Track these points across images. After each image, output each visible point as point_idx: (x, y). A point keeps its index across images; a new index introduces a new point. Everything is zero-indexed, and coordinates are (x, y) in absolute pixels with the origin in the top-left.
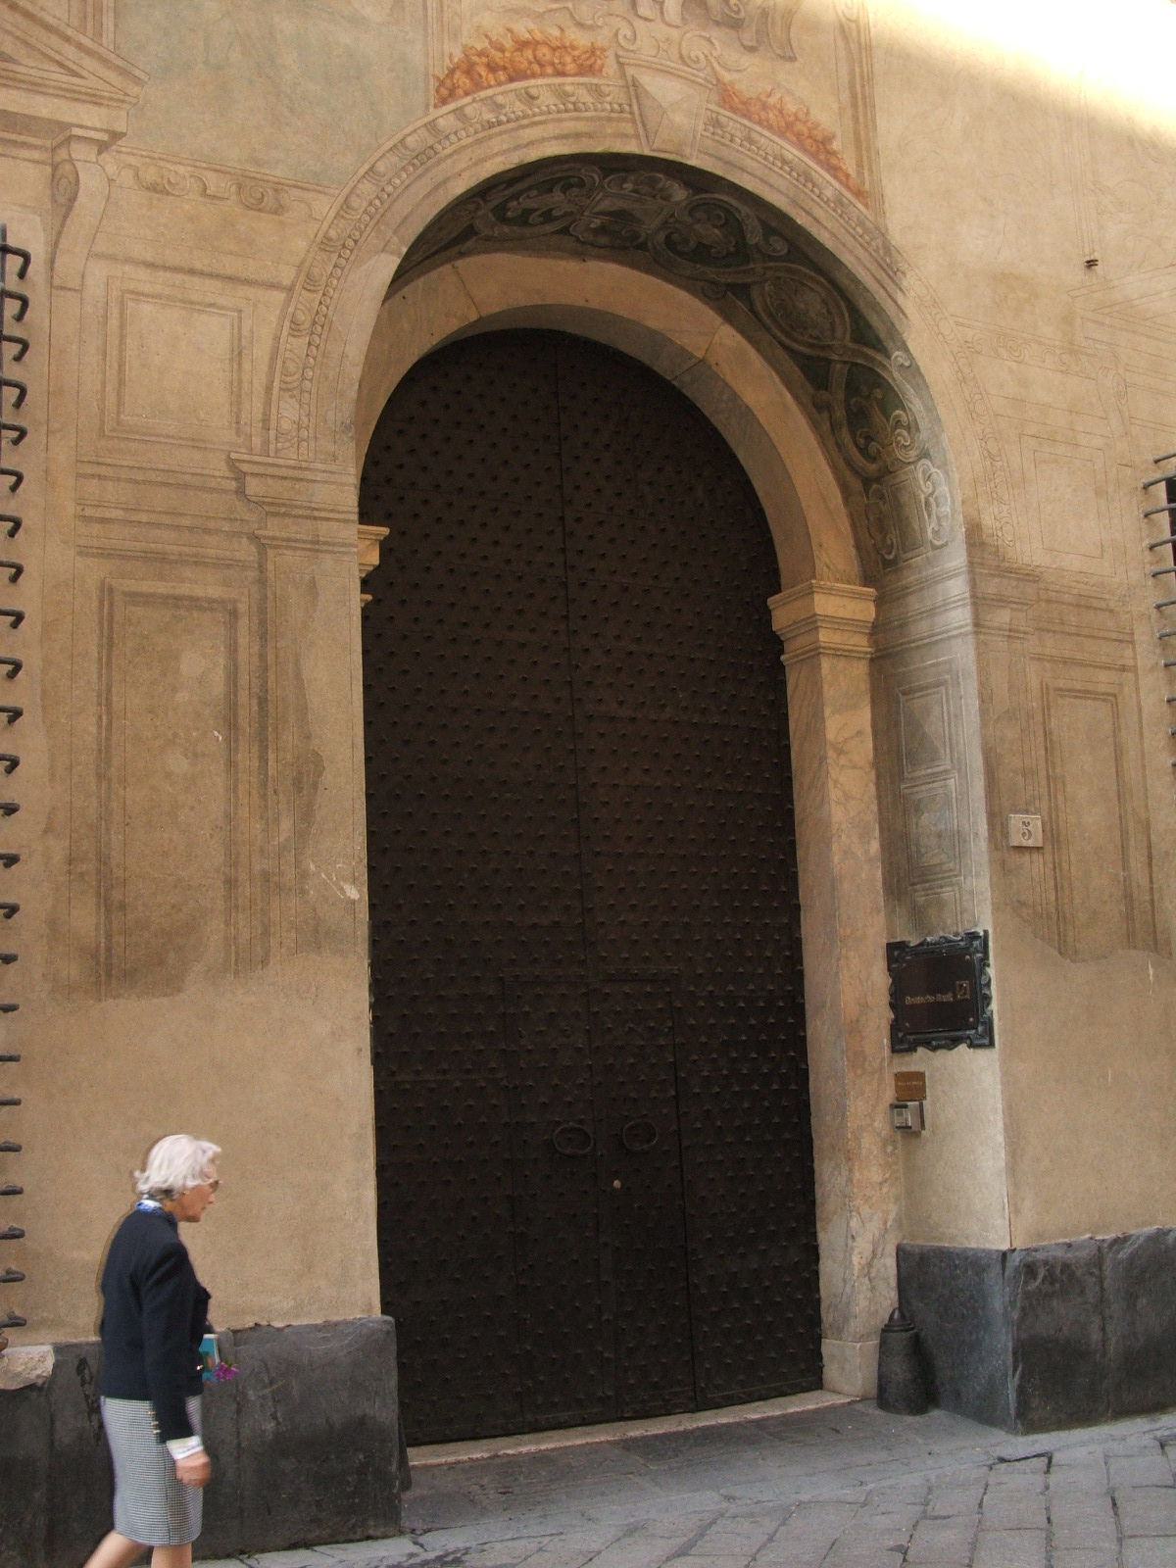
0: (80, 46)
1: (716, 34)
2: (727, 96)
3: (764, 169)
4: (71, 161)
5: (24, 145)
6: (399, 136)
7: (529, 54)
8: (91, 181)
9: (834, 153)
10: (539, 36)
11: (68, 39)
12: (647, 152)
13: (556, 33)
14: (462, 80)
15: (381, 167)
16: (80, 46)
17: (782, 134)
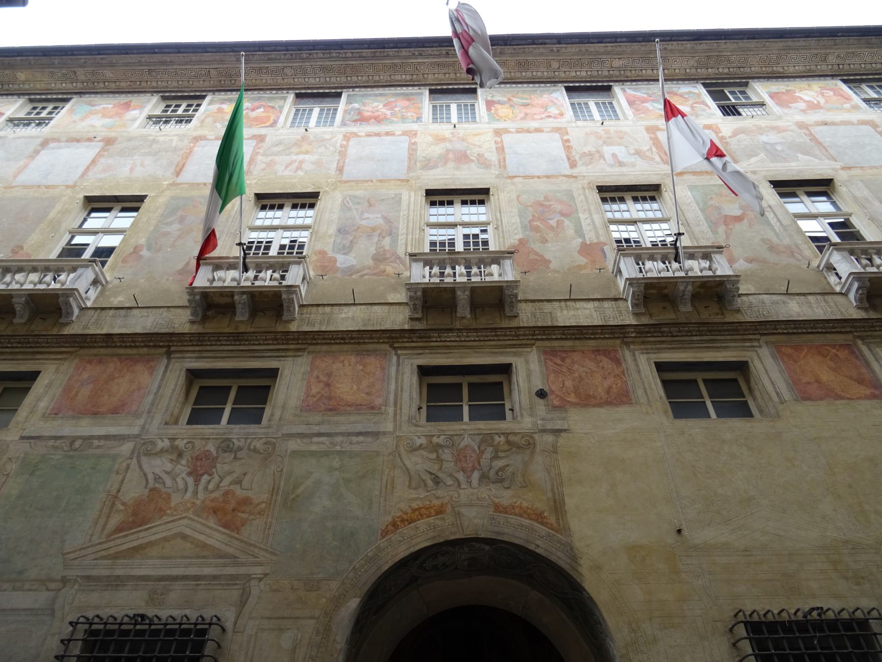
1: (492, 486)
2: (497, 508)
3: (515, 531)
5: (236, 584)
7: (417, 513)
8: (255, 592)
9: (545, 517)
10: (421, 506)
11: (256, 547)
12: (463, 537)
13: (428, 503)
14: (390, 527)
15: (357, 566)
16: (260, 548)
17: (521, 516)
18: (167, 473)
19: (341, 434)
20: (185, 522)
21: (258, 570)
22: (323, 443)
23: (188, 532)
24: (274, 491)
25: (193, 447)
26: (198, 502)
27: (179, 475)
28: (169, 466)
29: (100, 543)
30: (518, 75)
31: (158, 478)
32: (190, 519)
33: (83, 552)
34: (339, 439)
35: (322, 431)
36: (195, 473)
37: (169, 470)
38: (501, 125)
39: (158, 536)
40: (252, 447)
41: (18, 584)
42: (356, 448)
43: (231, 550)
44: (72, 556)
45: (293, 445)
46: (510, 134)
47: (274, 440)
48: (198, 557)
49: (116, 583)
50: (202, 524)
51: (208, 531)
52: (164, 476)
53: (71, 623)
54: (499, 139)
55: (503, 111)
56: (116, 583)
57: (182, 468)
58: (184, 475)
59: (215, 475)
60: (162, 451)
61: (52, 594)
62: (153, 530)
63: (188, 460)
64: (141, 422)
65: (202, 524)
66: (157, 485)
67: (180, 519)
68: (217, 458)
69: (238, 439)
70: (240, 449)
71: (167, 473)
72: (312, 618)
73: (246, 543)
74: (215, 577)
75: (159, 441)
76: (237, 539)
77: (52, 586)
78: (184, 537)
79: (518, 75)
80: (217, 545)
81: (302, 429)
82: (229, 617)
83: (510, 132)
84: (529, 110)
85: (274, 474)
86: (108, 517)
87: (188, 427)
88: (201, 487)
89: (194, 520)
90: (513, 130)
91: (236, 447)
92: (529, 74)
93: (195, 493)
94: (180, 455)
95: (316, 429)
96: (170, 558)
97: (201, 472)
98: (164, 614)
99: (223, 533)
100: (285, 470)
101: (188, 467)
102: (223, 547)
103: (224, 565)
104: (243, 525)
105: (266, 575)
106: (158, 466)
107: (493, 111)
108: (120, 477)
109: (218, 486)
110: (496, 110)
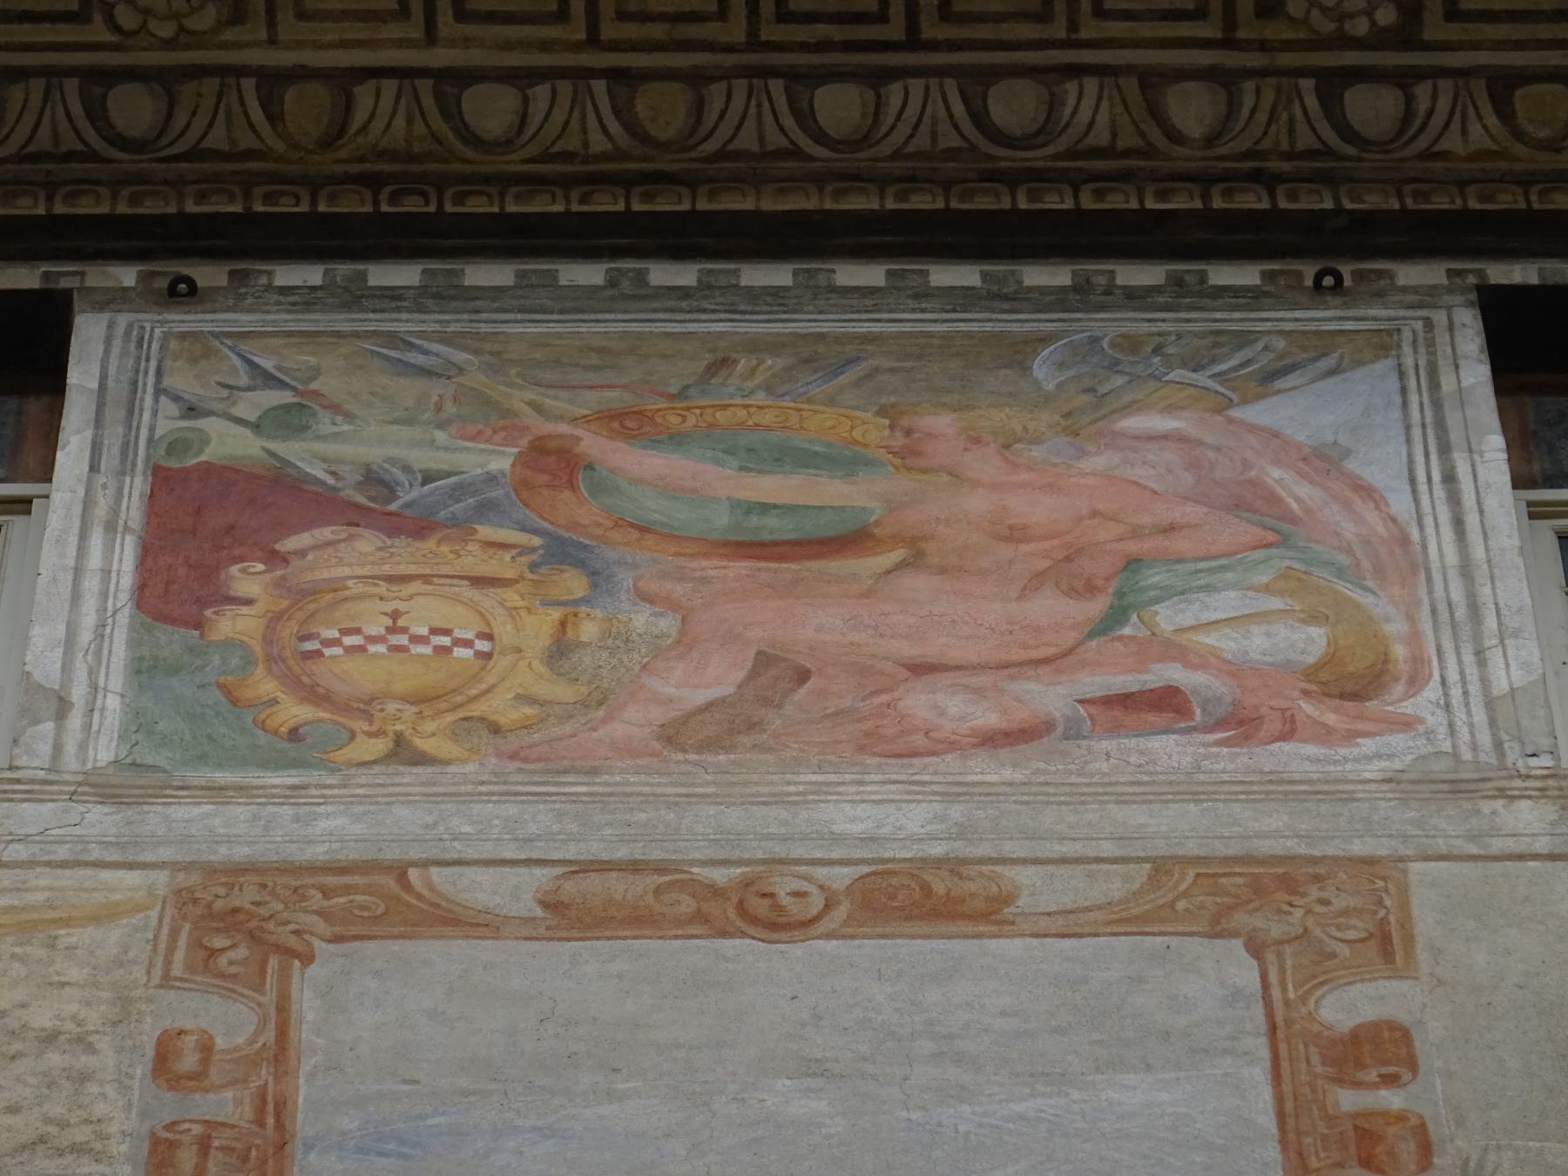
30: (748, 118)
38: (332, 822)
46: (442, 955)
54: (229, 1021)
55: (396, 616)
79: (748, 118)
83: (449, 919)
84: (820, 617)
90: (512, 893)
92: (923, 112)
107: (232, 625)
110: (302, 599)
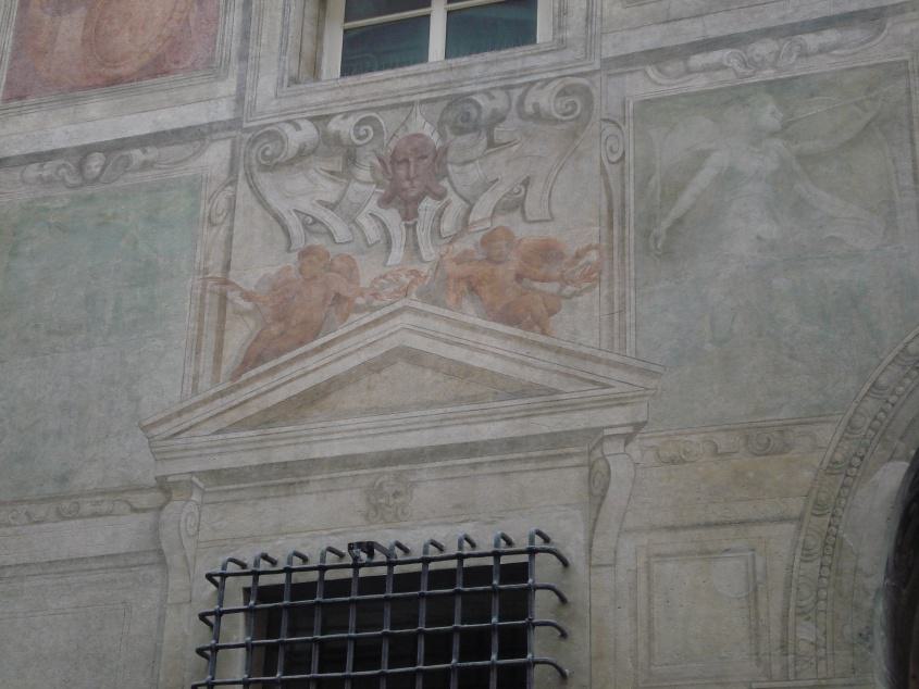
0: (608, 363)
4: (603, 457)
5: (568, 455)
6: (901, 346)
8: (620, 469)
11: (599, 361)
15: (883, 381)
16: (608, 363)
18: (332, 207)
19: (768, 32)
20: (407, 319)
21: (617, 417)
22: (721, 67)
23: (418, 343)
24: (613, 215)
25: (378, 131)
26: (425, 269)
27: (360, 207)
28: (329, 190)
29: (221, 394)
31: (311, 224)
32: (417, 312)
33: (188, 419)
34: (763, 49)
35: (713, 33)
36: (400, 198)
37: (331, 197)
39: (352, 362)
40: (529, 109)
41: (66, 504)
42: (820, 66)
43: (536, 376)
44: (164, 430)
45: (643, 85)
47: (583, 81)
48: (459, 400)
49: (288, 477)
50: (448, 320)
51: (467, 335)
52: (327, 216)
53: (210, 577)
56: (288, 477)
57: (364, 187)
58: (372, 206)
59: (452, 196)
60: (302, 154)
61: (148, 518)
62: (335, 348)
63: (373, 168)
64: (228, 87)
65: (448, 320)
66: (316, 241)
67: (392, 315)
68: (445, 151)
69: (486, 92)
70: (498, 118)
71: (332, 207)
72: (782, 520)
73: (569, 353)
74: (513, 444)
75: (288, 129)
76: (542, 346)
77: (143, 500)
78: (414, 357)
80: (498, 366)
81: (652, 38)
82: (569, 535)
85: (604, 172)
86: (221, 331)
87: (350, 80)
88: (423, 233)
89: (426, 315)
91: (486, 114)
93: (413, 248)
94: (351, 158)
95: (695, 30)
96: (393, 410)
97: (413, 194)
98: (416, 540)
99: (508, 337)
100: (630, 158)
101: (378, 184)
102: (514, 370)
103: (529, 414)
104: (552, 312)
105: (638, 426)
106: (306, 192)
108: (222, 233)
109: (465, 223)
